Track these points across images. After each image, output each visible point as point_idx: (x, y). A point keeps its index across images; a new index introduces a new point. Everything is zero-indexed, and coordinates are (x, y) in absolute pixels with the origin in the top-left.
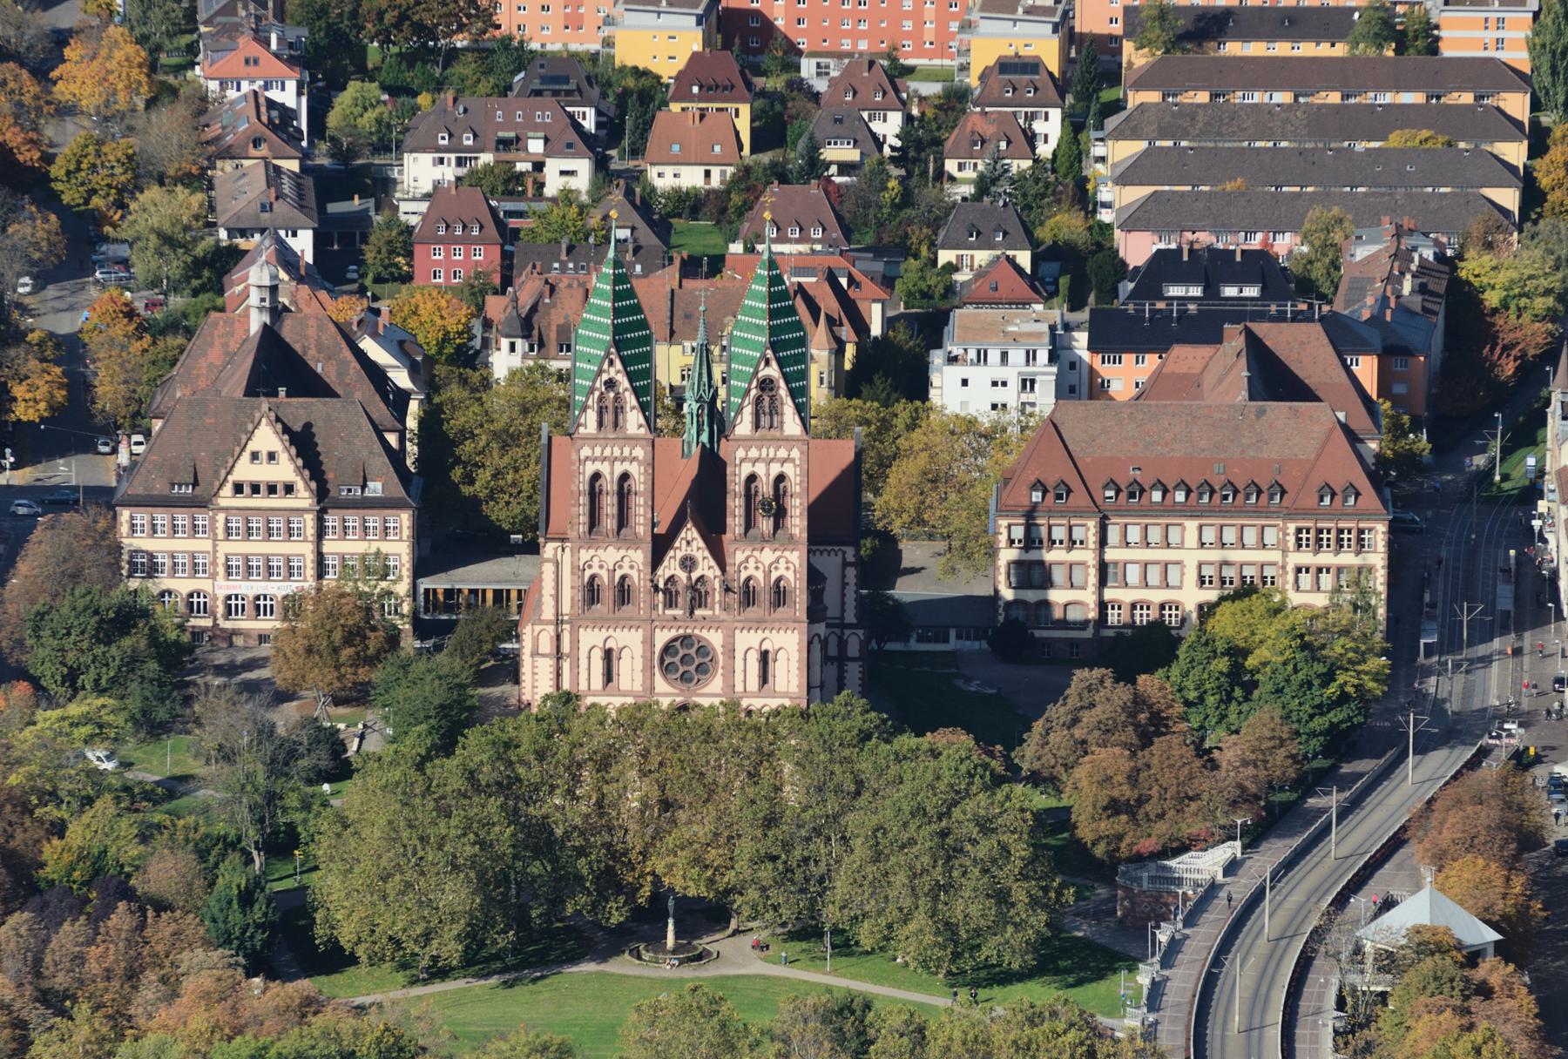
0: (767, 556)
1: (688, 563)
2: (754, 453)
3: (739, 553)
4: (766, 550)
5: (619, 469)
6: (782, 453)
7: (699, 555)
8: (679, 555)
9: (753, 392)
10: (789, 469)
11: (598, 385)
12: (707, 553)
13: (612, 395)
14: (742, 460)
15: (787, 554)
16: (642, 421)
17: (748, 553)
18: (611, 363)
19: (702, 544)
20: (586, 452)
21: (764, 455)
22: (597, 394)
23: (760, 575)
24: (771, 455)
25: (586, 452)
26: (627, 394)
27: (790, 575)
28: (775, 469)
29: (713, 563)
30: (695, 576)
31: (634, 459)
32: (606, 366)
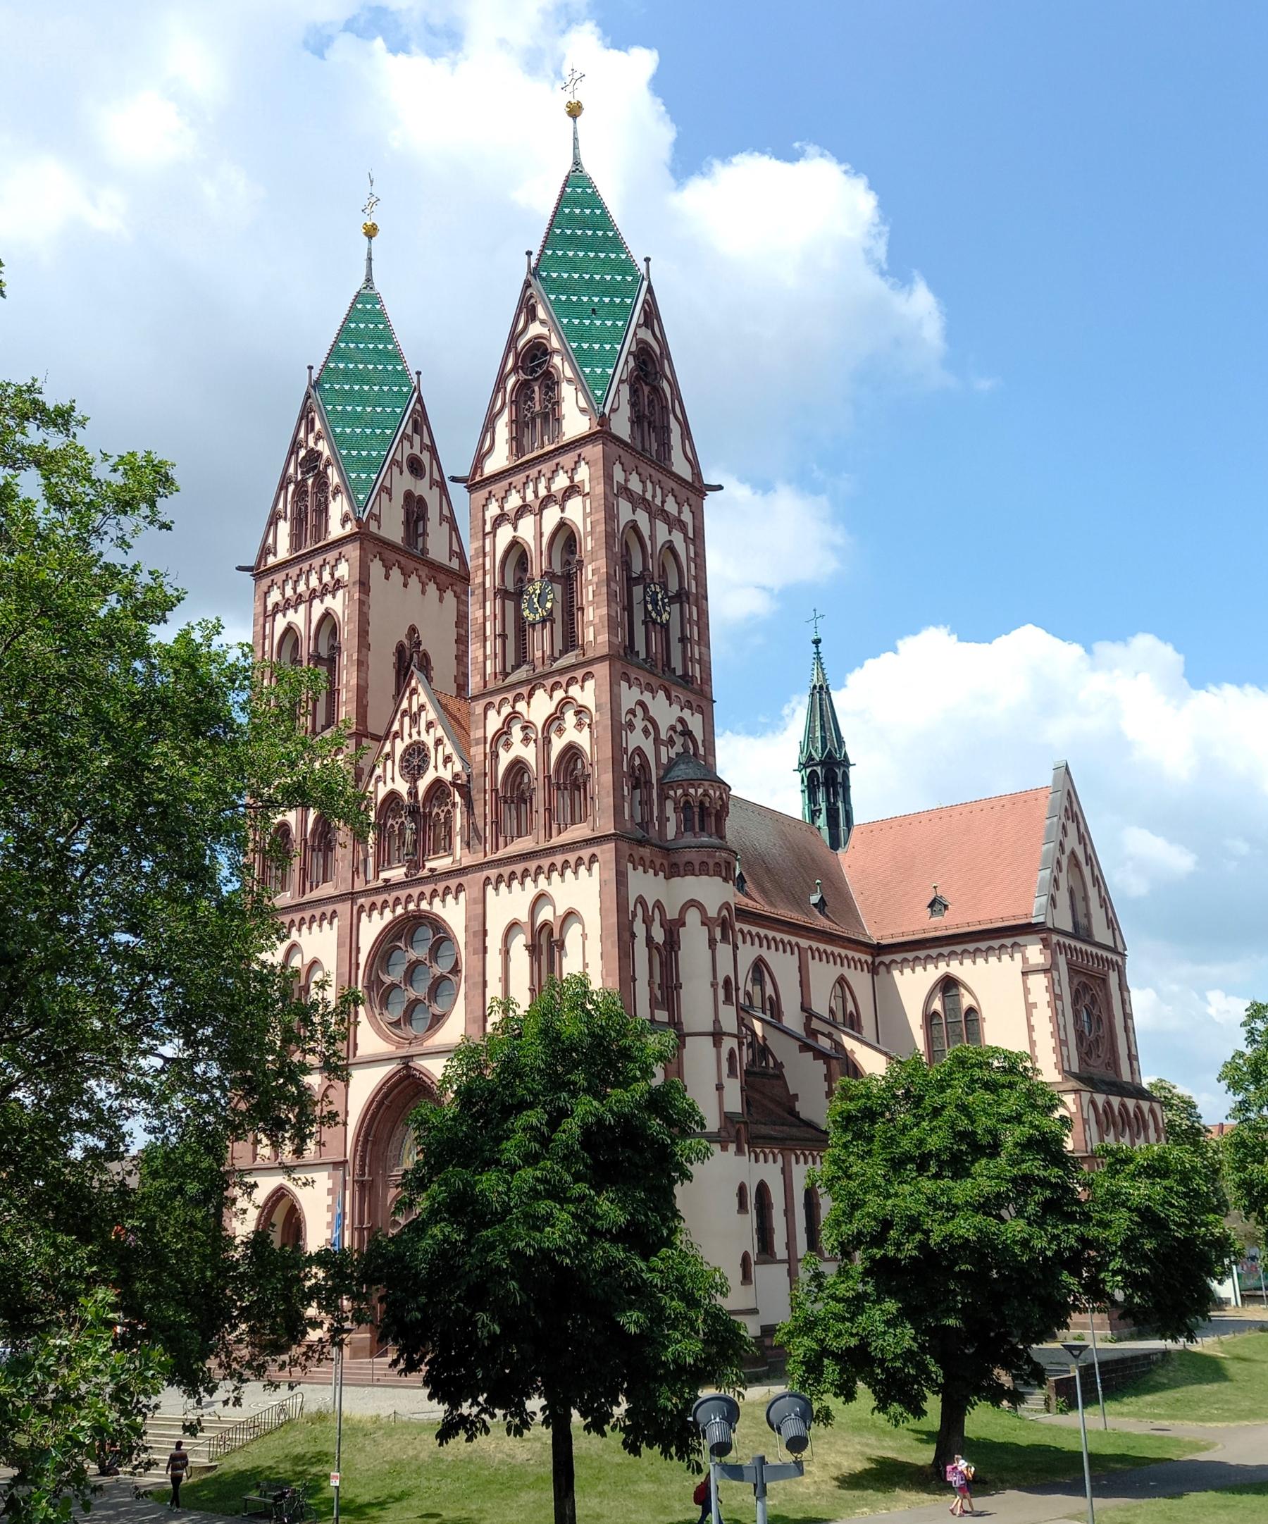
0: (540, 707)
1: (416, 759)
2: (514, 501)
3: (492, 714)
4: (540, 694)
5: (318, 609)
6: (562, 481)
7: (429, 740)
8: (400, 746)
9: (511, 382)
10: (575, 511)
11: (291, 470)
12: (440, 732)
13: (310, 482)
14: (499, 520)
15: (574, 691)
16: (346, 508)
17: (506, 710)
18: (310, 427)
19: (430, 714)
20: (275, 596)
21: (530, 496)
22: (291, 488)
23: (529, 754)
24: (543, 492)
25: (275, 596)
26: (329, 471)
27: (583, 739)
28: (552, 516)
29: (448, 748)
30: (423, 785)
31: (338, 584)
32: (302, 434)
